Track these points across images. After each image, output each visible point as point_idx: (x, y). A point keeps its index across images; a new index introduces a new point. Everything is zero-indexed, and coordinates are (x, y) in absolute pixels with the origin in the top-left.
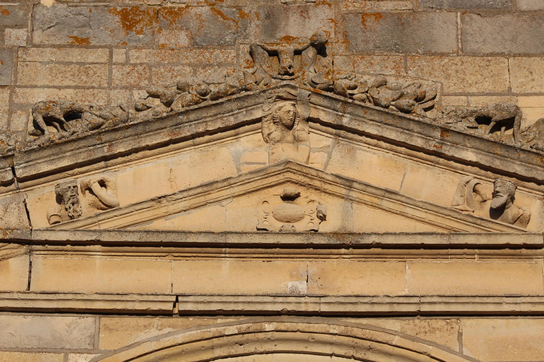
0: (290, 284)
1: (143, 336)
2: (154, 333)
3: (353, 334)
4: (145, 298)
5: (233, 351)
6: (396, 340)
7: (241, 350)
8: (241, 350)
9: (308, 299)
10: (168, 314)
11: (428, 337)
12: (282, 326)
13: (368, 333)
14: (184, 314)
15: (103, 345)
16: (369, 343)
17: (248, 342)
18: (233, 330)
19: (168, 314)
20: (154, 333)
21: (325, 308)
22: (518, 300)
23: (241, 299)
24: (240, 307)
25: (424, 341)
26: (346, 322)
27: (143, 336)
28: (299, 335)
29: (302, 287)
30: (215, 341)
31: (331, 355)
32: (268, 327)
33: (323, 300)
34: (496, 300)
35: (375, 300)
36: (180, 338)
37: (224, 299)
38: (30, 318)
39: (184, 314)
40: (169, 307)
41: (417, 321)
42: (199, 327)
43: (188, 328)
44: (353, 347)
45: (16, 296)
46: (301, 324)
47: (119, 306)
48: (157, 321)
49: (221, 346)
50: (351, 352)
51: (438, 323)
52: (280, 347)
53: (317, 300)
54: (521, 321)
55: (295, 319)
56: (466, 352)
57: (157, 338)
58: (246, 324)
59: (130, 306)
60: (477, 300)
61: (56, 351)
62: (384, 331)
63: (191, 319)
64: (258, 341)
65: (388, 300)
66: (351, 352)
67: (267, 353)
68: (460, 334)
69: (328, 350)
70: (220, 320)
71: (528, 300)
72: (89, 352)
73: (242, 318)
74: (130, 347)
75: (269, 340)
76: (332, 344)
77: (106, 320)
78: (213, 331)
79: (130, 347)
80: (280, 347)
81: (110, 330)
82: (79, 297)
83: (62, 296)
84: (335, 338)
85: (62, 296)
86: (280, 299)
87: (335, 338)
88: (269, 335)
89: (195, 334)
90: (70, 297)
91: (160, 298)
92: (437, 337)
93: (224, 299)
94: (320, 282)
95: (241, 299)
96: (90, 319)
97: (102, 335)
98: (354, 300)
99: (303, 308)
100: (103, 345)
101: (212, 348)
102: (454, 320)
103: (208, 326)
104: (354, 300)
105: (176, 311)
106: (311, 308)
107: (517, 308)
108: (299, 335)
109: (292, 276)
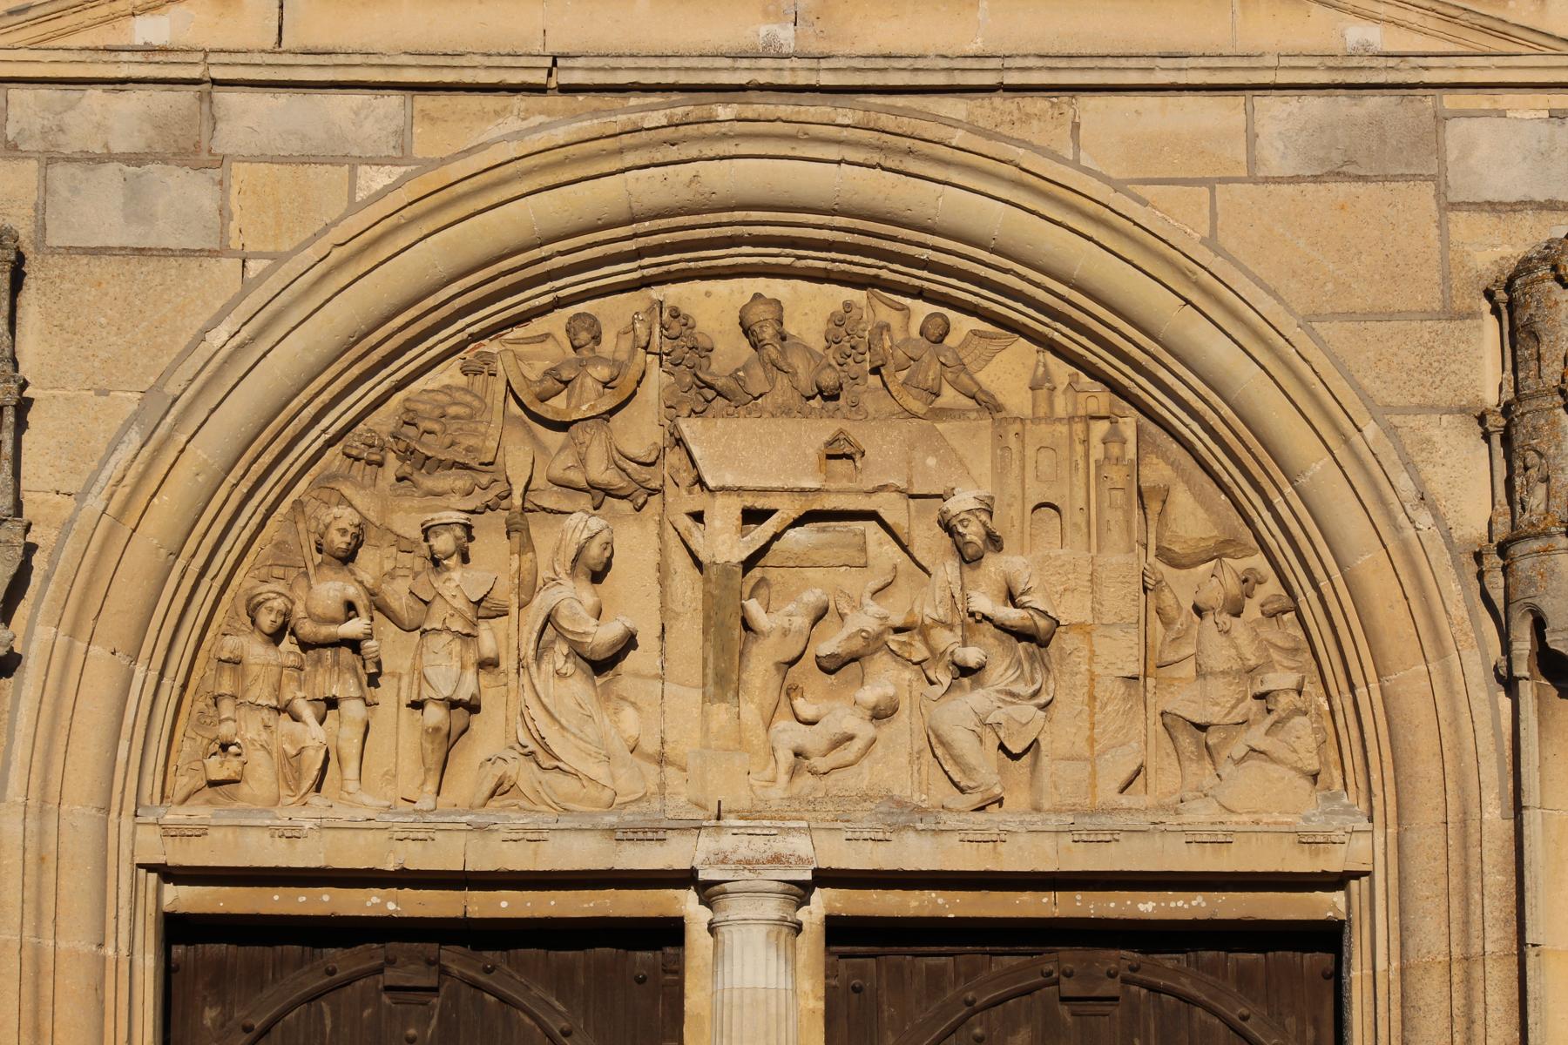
0: (763, 30)
1: (493, 131)
2: (513, 124)
3: (880, 125)
4: (496, 61)
5: (659, 157)
6: (959, 137)
7: (673, 153)
8: (673, 153)
9: (796, 63)
10: (540, 89)
11: (1017, 133)
12: (749, 112)
13: (906, 124)
14: (566, 89)
15: (419, 151)
16: (908, 142)
17: (685, 139)
18: (658, 118)
19: (540, 89)
20: (513, 124)
21: (827, 79)
22: (1184, 63)
23: (673, 62)
24: (670, 78)
25: (1010, 140)
26: (866, 102)
27: (493, 131)
28: (779, 127)
29: (786, 36)
30: (626, 139)
31: (839, 163)
32: (723, 112)
33: (824, 64)
34: (1144, 63)
35: (920, 64)
36: (561, 134)
37: (641, 63)
38: (284, 98)
39: (566, 89)
40: (539, 78)
41: (997, 100)
42: (596, 113)
43: (575, 116)
44: (880, 149)
45: (257, 58)
46: (784, 108)
47: (449, 77)
48: (518, 101)
49: (636, 148)
50: (876, 158)
51: (1037, 104)
52: (745, 148)
53: (813, 64)
54: (1188, 99)
55: (773, 97)
56: (1085, 160)
57: (519, 135)
58: (682, 108)
59: (468, 77)
60: (1108, 63)
61: (334, 161)
62: (936, 119)
63: (581, 98)
64: (705, 138)
65: (944, 63)
66: (876, 158)
67: (722, 158)
68: (1076, 127)
69: (833, 152)
70: (634, 100)
71: (1202, 62)
72: (394, 162)
73: (675, 97)
74: (468, 152)
75: (725, 136)
76: (839, 142)
77: (423, 101)
78: (622, 120)
79: (468, 152)
80: (745, 148)
81: (433, 120)
82: (374, 60)
83: (342, 59)
84: (846, 133)
85: (342, 59)
86: (745, 63)
87: (846, 133)
88: (725, 128)
89: (589, 126)
90: (357, 59)
91: (523, 62)
92: (1033, 132)
93: (641, 63)
94: (819, 25)
95: (673, 62)
96: (394, 99)
97: (417, 130)
98: (881, 63)
99: (786, 79)
100: (419, 151)
101: (621, 151)
102: (1065, 98)
103: (612, 111)
104: (881, 63)
105: (553, 85)
106: (802, 79)
107: (1182, 79)
108: (779, 127)
109: (766, 14)
